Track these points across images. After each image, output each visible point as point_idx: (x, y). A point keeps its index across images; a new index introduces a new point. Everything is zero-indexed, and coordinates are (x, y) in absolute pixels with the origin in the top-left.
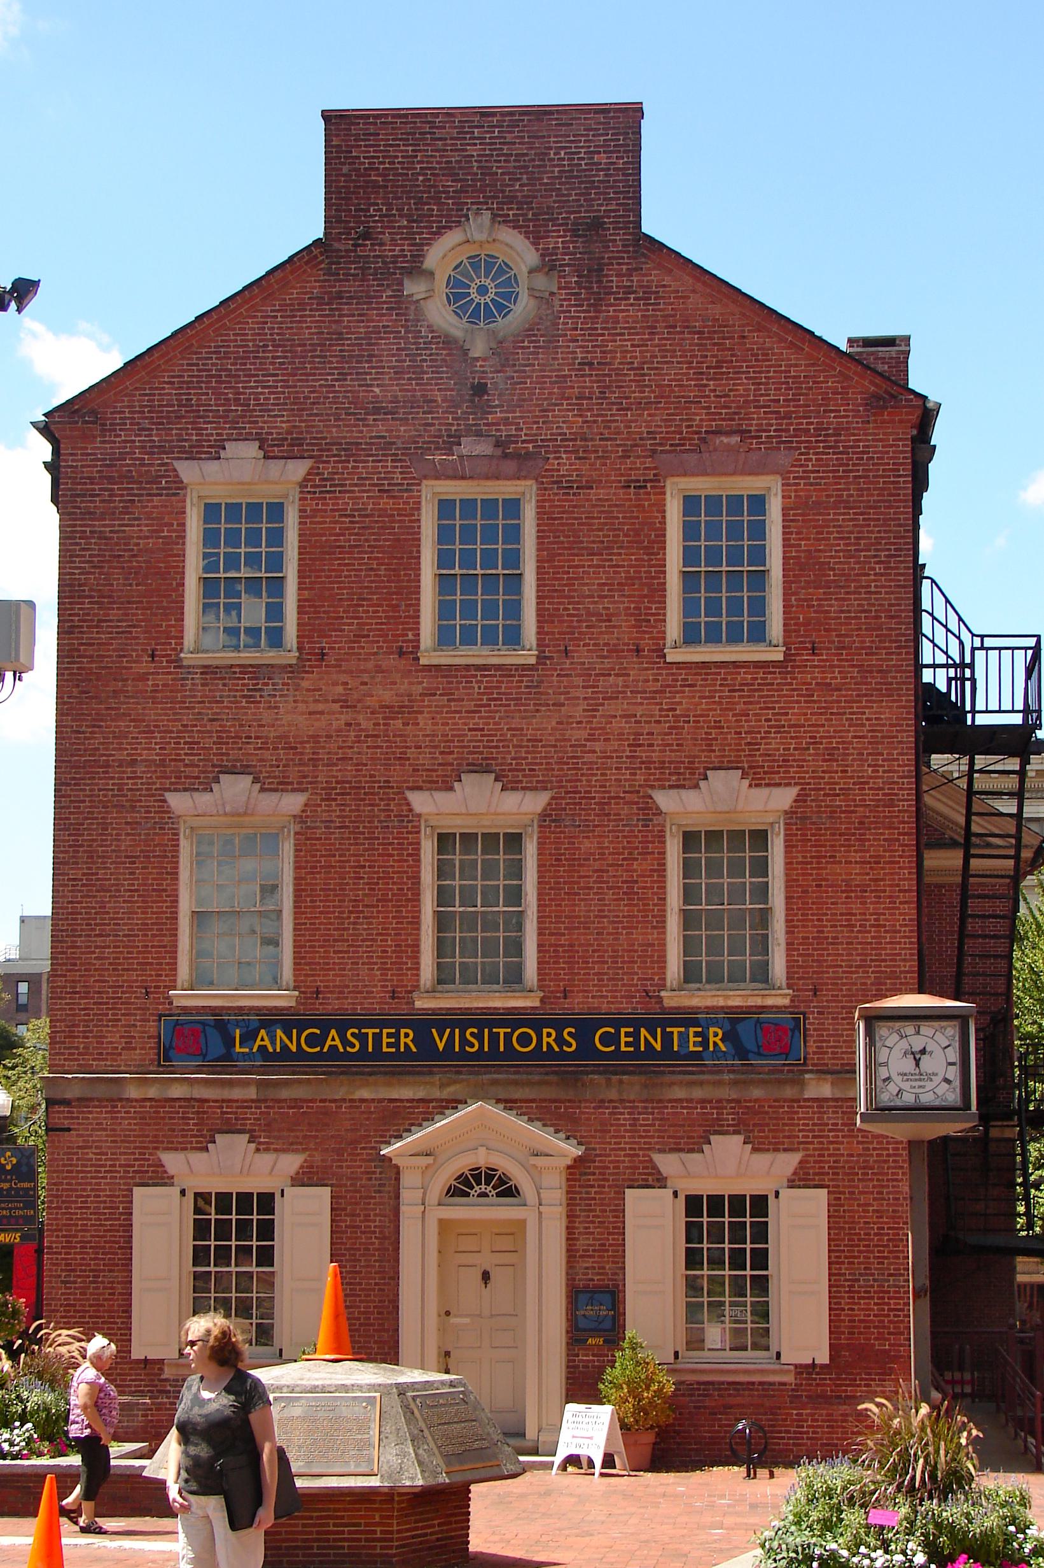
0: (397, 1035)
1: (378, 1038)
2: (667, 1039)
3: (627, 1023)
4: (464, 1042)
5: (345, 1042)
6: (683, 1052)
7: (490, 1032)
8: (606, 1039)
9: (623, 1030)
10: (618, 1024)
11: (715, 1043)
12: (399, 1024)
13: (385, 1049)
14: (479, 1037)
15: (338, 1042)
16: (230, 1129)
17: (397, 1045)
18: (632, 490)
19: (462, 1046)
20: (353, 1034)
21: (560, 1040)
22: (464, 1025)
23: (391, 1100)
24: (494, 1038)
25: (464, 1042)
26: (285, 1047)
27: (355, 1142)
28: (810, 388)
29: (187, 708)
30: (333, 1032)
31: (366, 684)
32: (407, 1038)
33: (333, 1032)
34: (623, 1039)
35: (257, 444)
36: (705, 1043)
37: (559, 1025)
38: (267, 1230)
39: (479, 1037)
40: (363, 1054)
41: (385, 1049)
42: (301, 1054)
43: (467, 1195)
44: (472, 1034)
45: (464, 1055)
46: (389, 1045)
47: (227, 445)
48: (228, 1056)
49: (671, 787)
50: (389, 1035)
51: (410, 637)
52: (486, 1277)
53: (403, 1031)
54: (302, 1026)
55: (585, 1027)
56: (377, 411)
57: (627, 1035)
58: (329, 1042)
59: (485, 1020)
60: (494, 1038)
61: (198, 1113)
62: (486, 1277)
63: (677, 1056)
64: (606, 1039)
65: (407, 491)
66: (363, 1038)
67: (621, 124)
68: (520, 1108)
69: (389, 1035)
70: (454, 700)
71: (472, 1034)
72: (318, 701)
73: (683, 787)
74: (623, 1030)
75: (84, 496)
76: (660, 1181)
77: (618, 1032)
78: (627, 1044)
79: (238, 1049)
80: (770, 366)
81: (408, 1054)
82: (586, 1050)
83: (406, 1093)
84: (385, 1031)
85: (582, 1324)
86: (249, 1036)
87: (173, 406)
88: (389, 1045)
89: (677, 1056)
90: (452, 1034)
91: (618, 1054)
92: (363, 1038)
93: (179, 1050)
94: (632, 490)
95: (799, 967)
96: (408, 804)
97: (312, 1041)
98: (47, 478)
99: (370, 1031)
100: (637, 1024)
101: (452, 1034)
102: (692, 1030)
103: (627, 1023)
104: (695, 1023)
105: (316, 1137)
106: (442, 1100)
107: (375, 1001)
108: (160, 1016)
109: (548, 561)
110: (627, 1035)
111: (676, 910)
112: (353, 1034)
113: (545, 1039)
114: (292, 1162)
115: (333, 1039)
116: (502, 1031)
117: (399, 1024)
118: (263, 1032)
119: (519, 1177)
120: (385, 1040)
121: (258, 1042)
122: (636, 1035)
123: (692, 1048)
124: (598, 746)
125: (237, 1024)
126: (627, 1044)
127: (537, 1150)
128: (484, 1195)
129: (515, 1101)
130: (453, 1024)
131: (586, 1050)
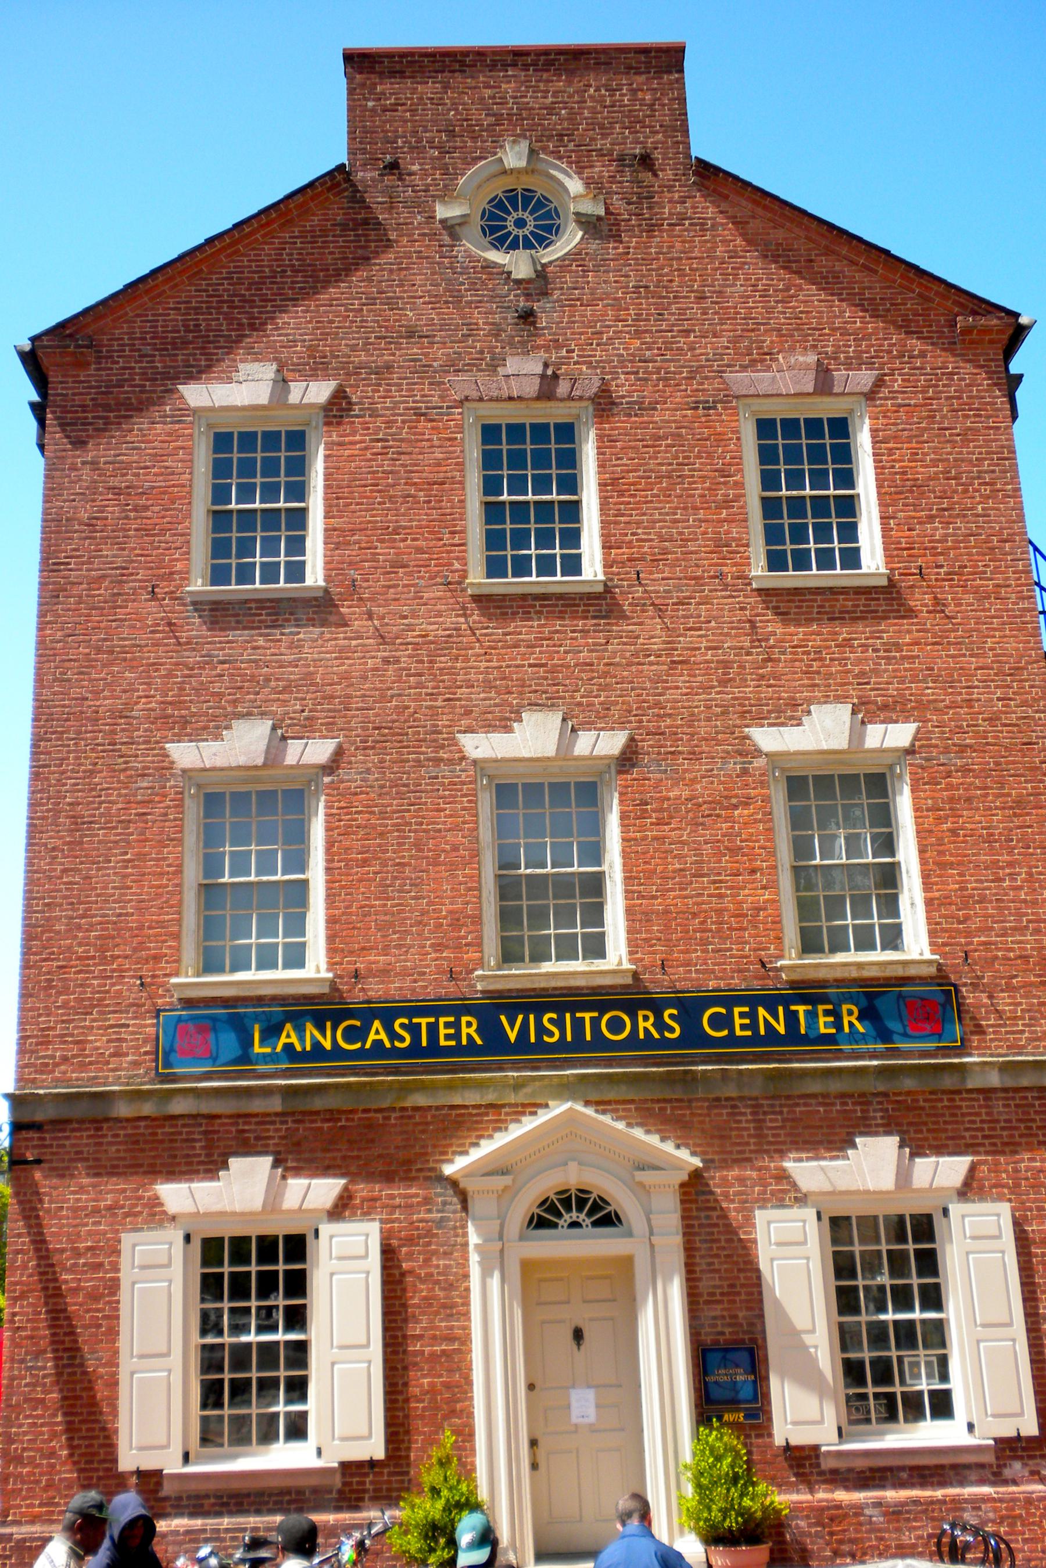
0: (457, 1025)
1: (433, 1029)
2: (792, 1018)
3: (740, 1001)
4: (541, 1030)
5: (393, 1036)
6: (812, 1035)
7: (573, 1018)
8: (717, 1022)
9: (737, 1010)
10: (729, 1002)
11: (851, 1024)
12: (458, 1011)
13: (443, 1042)
14: (560, 1024)
15: (383, 1036)
16: (248, 1148)
17: (457, 1036)
18: (701, 412)
19: (539, 1036)
20: (402, 1025)
21: (660, 1025)
22: (540, 1009)
23: (452, 1107)
24: (578, 1024)
25: (541, 1030)
26: (317, 1045)
27: (409, 1162)
28: (888, 310)
29: (194, 650)
30: (377, 1024)
31: (405, 617)
32: (469, 1029)
33: (377, 1024)
34: (738, 1021)
35: (275, 367)
36: (838, 1024)
37: (656, 1007)
38: (298, 1284)
39: (560, 1024)
40: (415, 1049)
41: (443, 1042)
42: (337, 1052)
43: (555, 1226)
44: (550, 1020)
45: (540, 1047)
46: (448, 1037)
47: (241, 366)
48: (245, 1057)
49: (771, 725)
50: (447, 1025)
51: (457, 566)
52: (578, 1335)
53: (464, 1019)
54: (338, 1016)
55: (689, 1008)
56: (411, 334)
57: (742, 1015)
58: (372, 1037)
59: (566, 1000)
60: (578, 1024)
61: (205, 1133)
62: (578, 1335)
63: (805, 1040)
64: (717, 1022)
65: (448, 414)
66: (414, 1030)
67: (663, 62)
68: (616, 1111)
69: (447, 1025)
70: (509, 634)
71: (550, 1020)
72: (351, 639)
73: (782, 724)
74: (737, 1010)
75: (75, 424)
76: (802, 1199)
77: (730, 1013)
78: (743, 1027)
79: (257, 1049)
80: (843, 289)
81: (471, 1048)
82: (693, 1036)
83: (471, 1098)
84: (442, 1020)
85: (716, 1393)
86: (272, 1032)
87: (179, 331)
88: (448, 1037)
89: (805, 1040)
90: (525, 1024)
91: (732, 1040)
92: (414, 1030)
93: (183, 1053)
94: (701, 412)
95: (943, 930)
96: (461, 751)
97: (351, 1035)
98: (33, 424)
99: (424, 1021)
100: (753, 1002)
101: (525, 1024)
102: (821, 1008)
103: (740, 1001)
104: (824, 999)
105: (358, 1157)
106: (516, 1105)
107: (430, 986)
108: (158, 1011)
109: (612, 484)
110: (742, 1015)
111: (787, 866)
112: (402, 1025)
113: (642, 1024)
114: (325, 1190)
115: (377, 1033)
116: (587, 1016)
117: (458, 1011)
118: (288, 1026)
119: (622, 1199)
120: (442, 1031)
121: (283, 1040)
122: (753, 1015)
123: (823, 1030)
124: (680, 681)
125: (256, 1017)
126: (743, 1027)
127: (651, 1158)
128: (575, 1225)
129: (609, 1103)
130: (526, 1008)
131: (693, 1036)
